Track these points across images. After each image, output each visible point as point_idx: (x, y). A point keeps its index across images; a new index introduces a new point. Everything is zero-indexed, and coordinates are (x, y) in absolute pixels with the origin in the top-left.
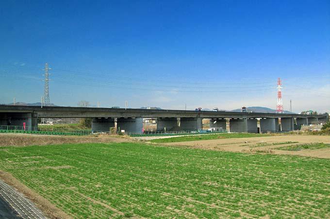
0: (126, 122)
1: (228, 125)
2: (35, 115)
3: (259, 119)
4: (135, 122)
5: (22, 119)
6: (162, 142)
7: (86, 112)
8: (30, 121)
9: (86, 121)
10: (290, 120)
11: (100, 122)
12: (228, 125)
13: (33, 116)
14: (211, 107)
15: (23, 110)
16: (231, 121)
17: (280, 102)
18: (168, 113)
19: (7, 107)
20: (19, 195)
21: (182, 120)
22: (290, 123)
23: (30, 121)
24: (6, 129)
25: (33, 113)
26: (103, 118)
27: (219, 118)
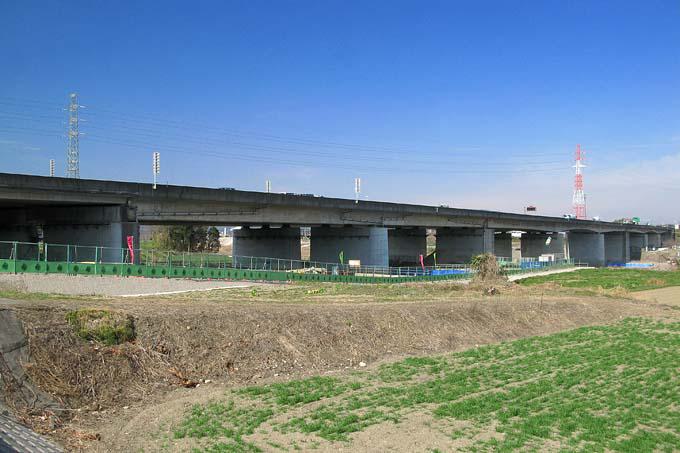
0: (342, 237)
1: (516, 246)
2: (131, 213)
3: (517, 234)
4: (368, 237)
5: (87, 225)
6: (579, 287)
7: (264, 206)
8: (117, 230)
9: (171, 235)
10: (621, 238)
11: (259, 238)
12: (516, 246)
13: (125, 218)
14: (155, 172)
15: (101, 193)
16: (523, 238)
17: (578, 199)
18: (320, 208)
19: (70, 186)
20: (18, 436)
21: (443, 234)
22: (621, 245)
23: (117, 230)
24: (42, 260)
25: (126, 205)
26: (266, 226)
27: (537, 232)
